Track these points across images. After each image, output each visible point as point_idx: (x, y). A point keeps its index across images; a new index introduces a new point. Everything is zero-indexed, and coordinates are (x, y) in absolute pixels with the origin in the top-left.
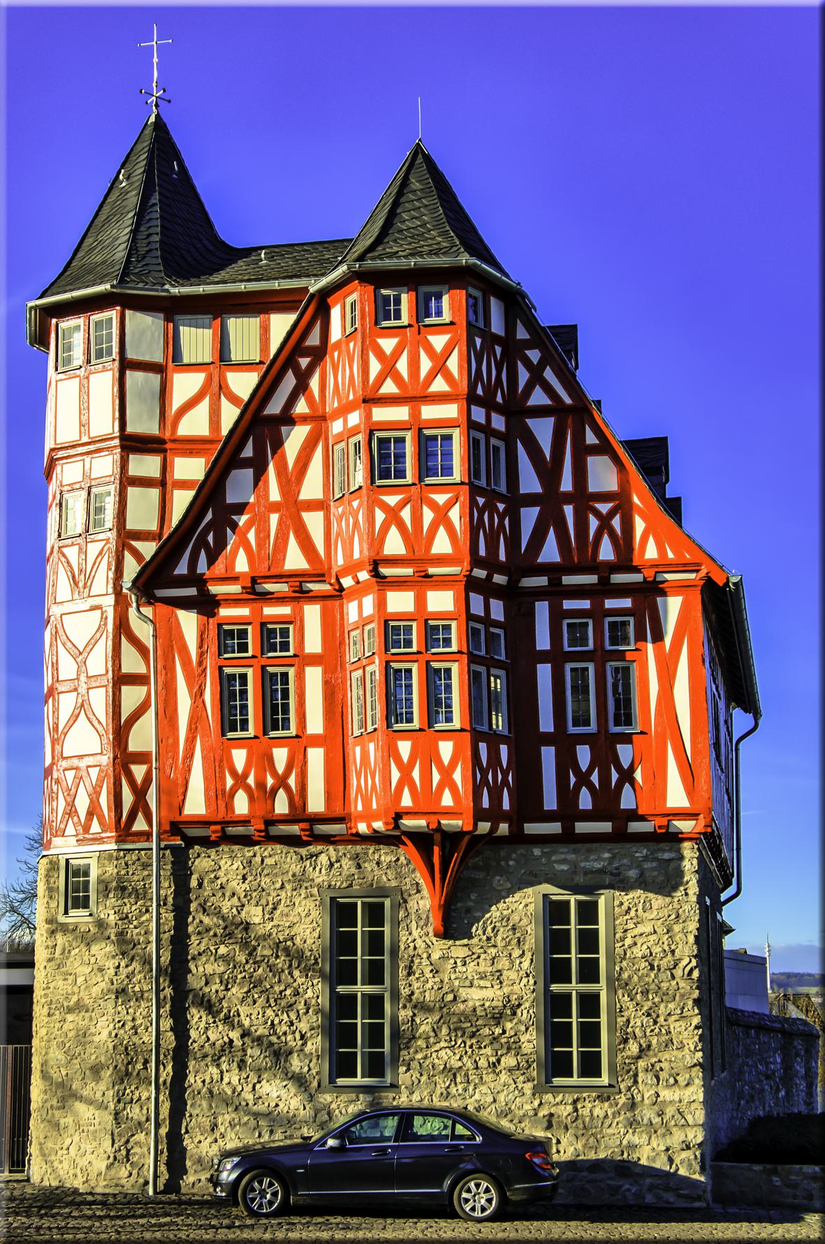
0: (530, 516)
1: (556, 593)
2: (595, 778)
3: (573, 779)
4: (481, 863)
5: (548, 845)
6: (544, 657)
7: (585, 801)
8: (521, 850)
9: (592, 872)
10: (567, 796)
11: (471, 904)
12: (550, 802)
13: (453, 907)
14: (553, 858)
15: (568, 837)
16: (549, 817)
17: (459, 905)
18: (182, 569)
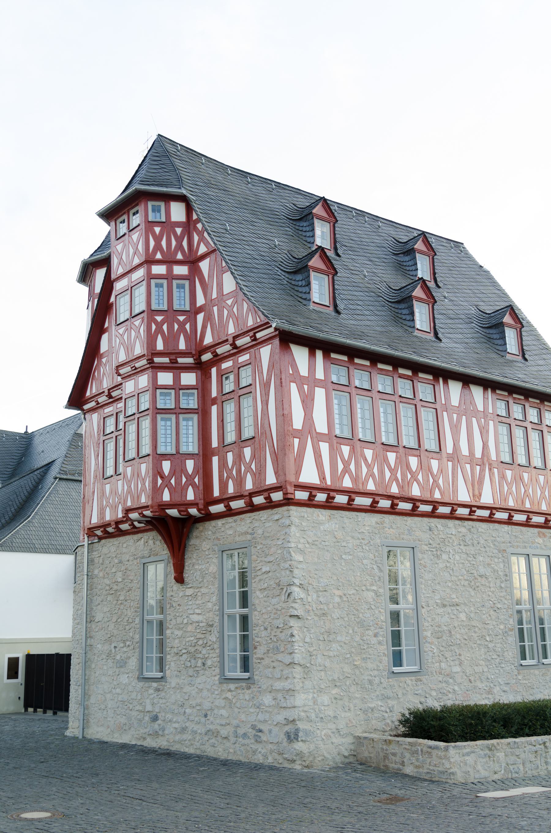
0: (200, 318)
1: (217, 360)
2: (234, 472)
3: (225, 475)
4: (198, 535)
5: (224, 519)
6: (214, 401)
7: (231, 490)
8: (213, 523)
9: (242, 534)
10: (223, 486)
11: (194, 561)
12: (216, 493)
13: (186, 564)
14: (227, 527)
15: (230, 513)
16: (217, 501)
17: (190, 562)
18: (88, 394)
